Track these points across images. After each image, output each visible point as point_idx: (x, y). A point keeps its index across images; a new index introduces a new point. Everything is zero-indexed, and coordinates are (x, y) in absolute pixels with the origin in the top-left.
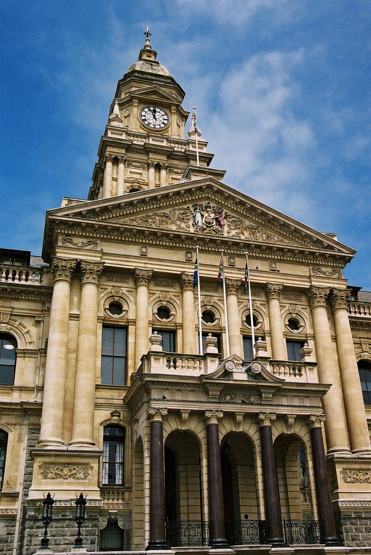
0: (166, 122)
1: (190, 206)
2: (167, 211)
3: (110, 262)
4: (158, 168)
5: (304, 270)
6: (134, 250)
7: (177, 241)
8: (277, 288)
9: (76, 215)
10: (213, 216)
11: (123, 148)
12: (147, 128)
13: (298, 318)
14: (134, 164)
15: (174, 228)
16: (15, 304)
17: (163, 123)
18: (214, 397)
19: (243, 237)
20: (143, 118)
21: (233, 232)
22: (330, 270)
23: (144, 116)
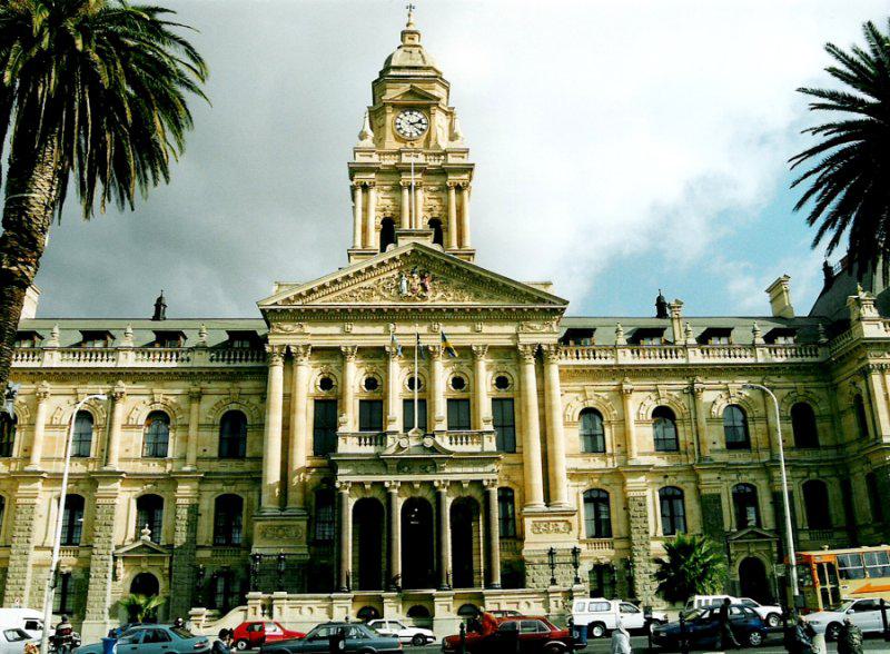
2: (369, 283)
6: (335, 329)
10: (418, 281)
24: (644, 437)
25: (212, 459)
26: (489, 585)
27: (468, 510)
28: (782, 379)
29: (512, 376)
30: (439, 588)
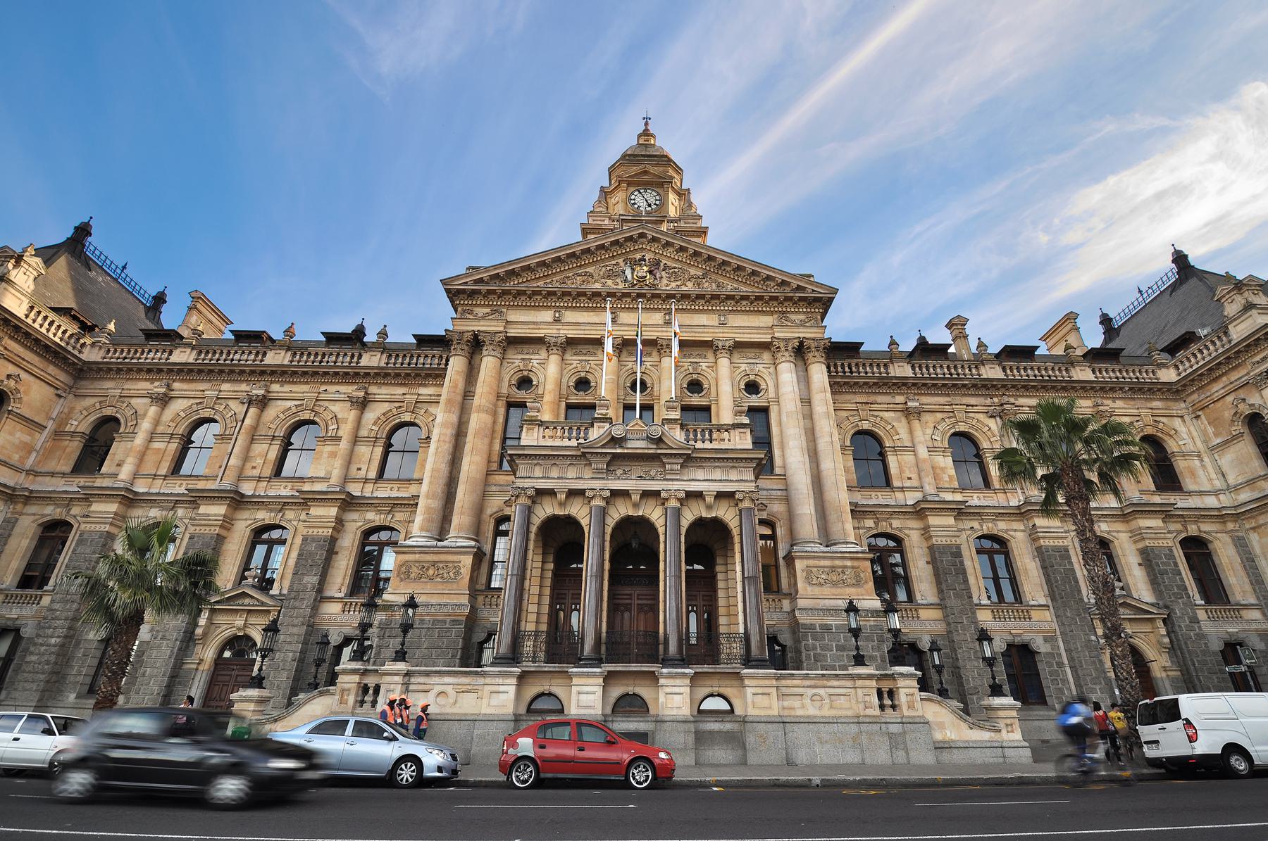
1: (621, 261)
2: (591, 270)
3: (513, 332)
5: (767, 320)
7: (595, 299)
8: (727, 344)
9: (477, 282)
13: (758, 380)
15: (598, 285)
16: (423, 391)
18: (598, 471)
19: (684, 288)
21: (673, 285)
22: (802, 317)
24: (943, 469)
25: (366, 480)
26: (748, 661)
27: (707, 543)
28: (1119, 403)
29: (767, 383)
30: (666, 662)
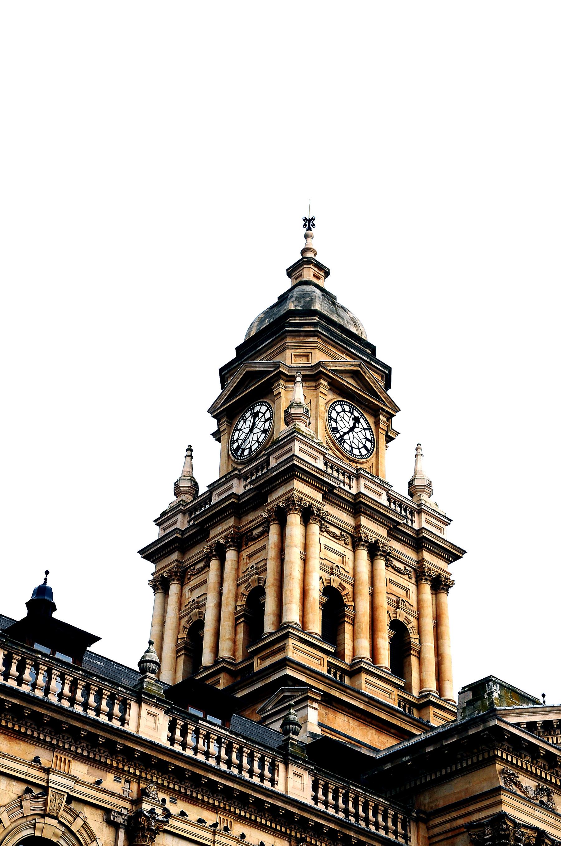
0: (369, 445)
4: (374, 551)
11: (319, 490)
12: (338, 449)
14: (331, 529)
17: (365, 447)
20: (334, 425)
23: (336, 421)
